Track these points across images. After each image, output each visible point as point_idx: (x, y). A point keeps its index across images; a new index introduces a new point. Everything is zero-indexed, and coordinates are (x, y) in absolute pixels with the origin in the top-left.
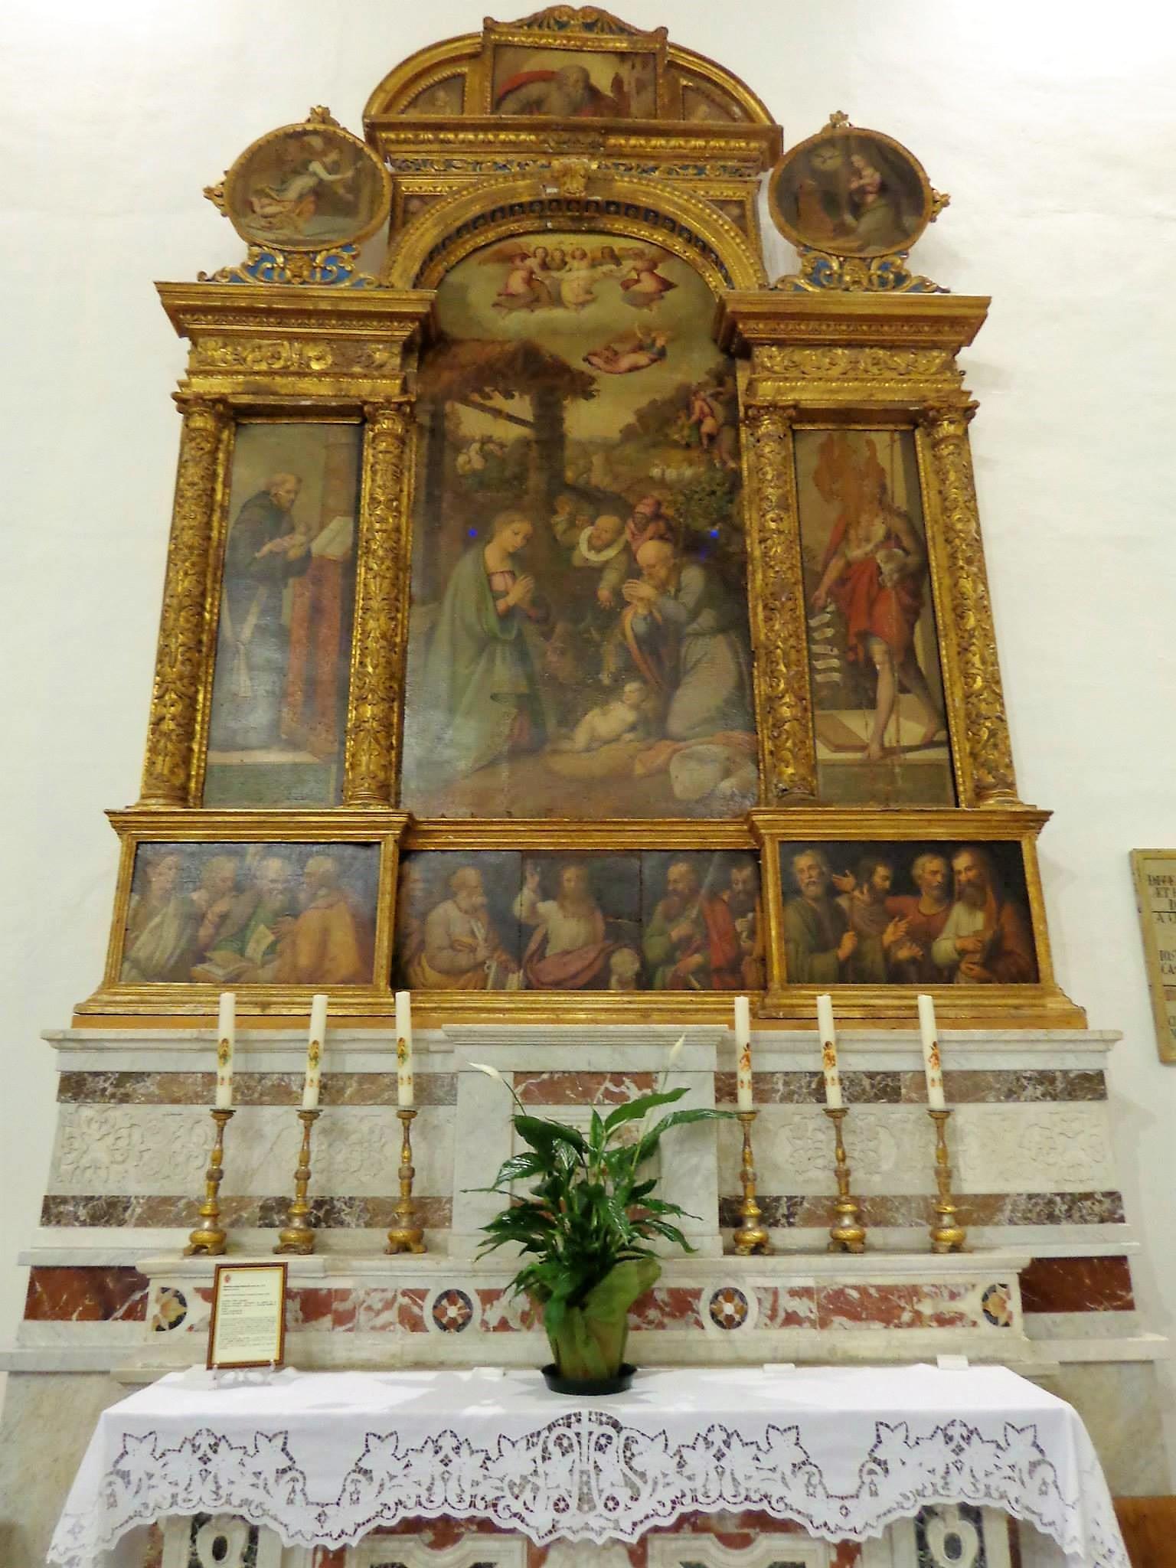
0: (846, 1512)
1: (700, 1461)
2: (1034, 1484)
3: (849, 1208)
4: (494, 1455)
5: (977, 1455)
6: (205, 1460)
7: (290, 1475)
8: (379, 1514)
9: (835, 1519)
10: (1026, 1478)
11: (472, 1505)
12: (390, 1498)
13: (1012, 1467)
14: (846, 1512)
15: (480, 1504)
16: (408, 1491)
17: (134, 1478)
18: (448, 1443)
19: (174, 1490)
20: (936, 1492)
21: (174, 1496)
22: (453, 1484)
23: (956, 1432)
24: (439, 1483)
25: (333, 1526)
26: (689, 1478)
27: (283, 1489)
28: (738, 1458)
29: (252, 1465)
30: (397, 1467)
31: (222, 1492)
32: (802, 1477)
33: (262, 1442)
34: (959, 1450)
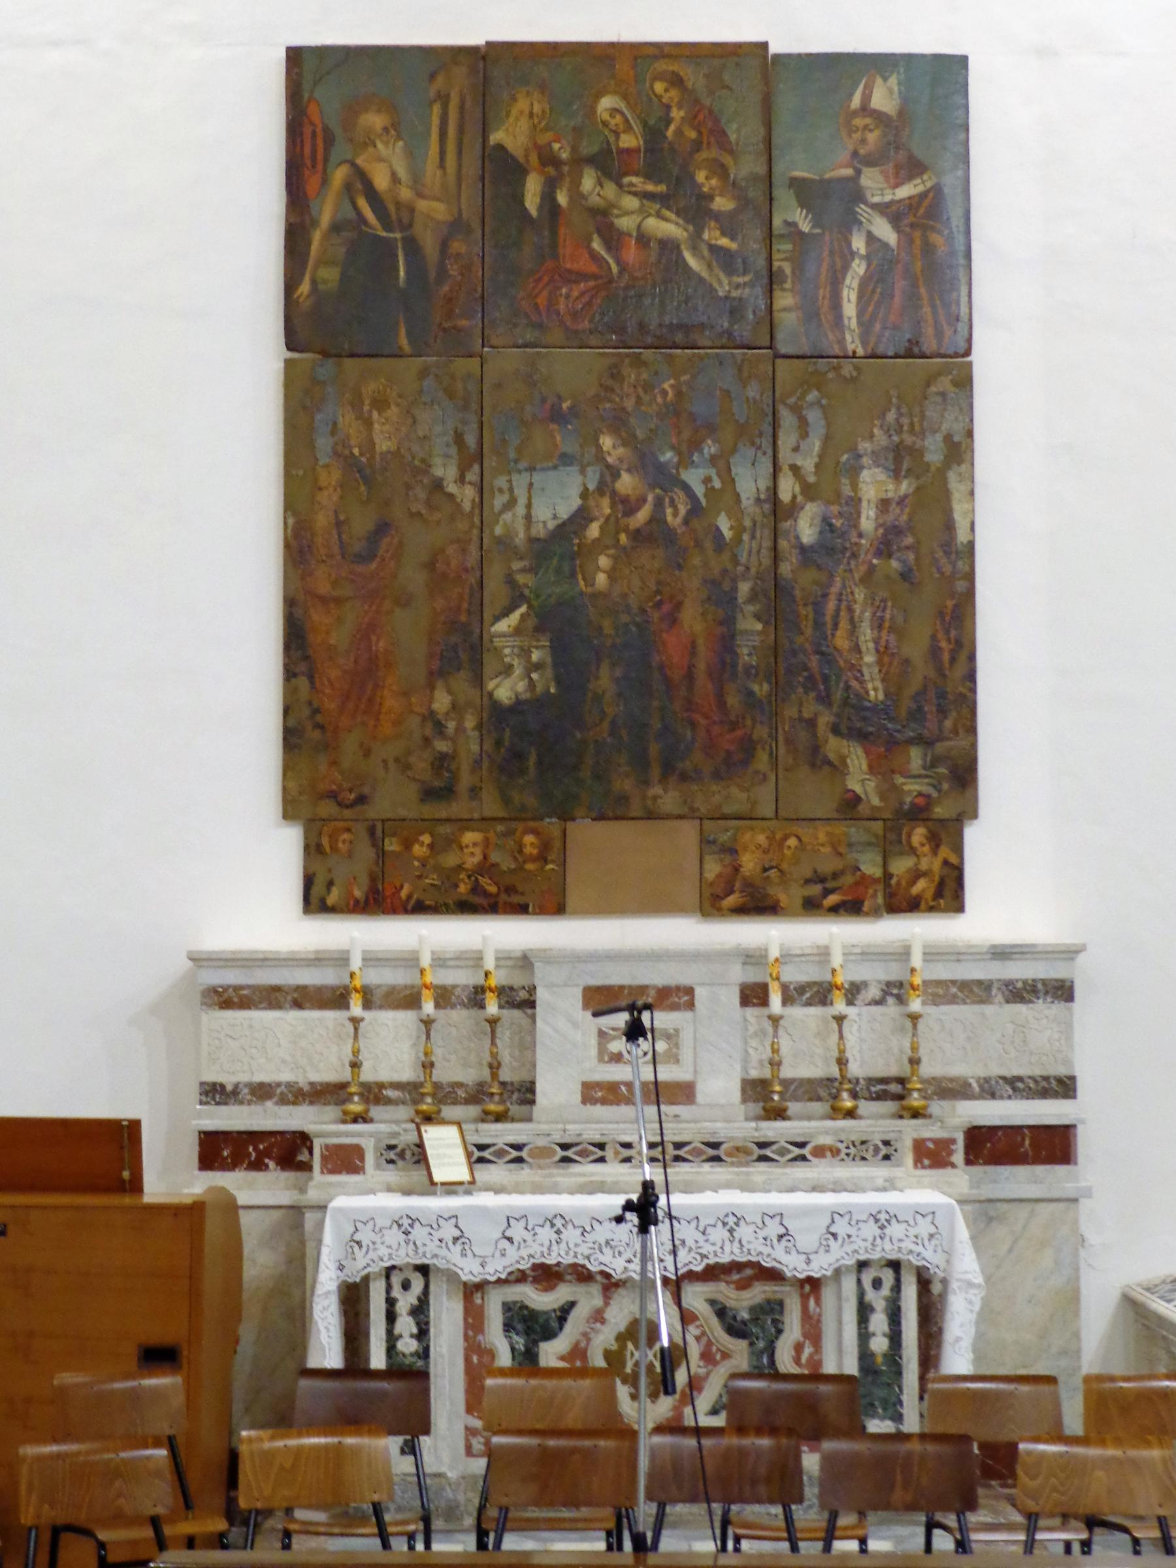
0: (808, 1262)
1: (719, 1234)
2: (930, 1248)
3: (846, 1086)
4: (588, 1228)
5: (895, 1230)
6: (406, 1233)
7: (463, 1240)
8: (518, 1262)
9: (801, 1265)
10: (926, 1242)
11: (576, 1256)
12: (524, 1253)
13: (916, 1237)
14: (808, 1262)
15: (579, 1256)
16: (535, 1249)
17: (364, 1244)
18: (559, 1222)
19: (390, 1251)
20: (867, 1251)
21: (390, 1255)
22: (563, 1245)
23: (883, 1217)
24: (555, 1247)
25: (490, 1269)
26: (714, 1244)
27: (458, 1248)
28: (744, 1232)
29: (437, 1235)
30: (528, 1236)
31: (420, 1251)
32: (784, 1242)
33: (441, 1221)
34: (882, 1227)
